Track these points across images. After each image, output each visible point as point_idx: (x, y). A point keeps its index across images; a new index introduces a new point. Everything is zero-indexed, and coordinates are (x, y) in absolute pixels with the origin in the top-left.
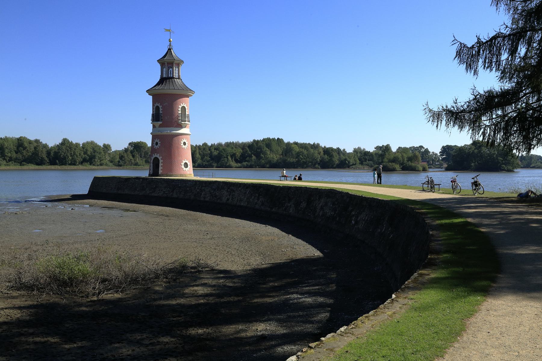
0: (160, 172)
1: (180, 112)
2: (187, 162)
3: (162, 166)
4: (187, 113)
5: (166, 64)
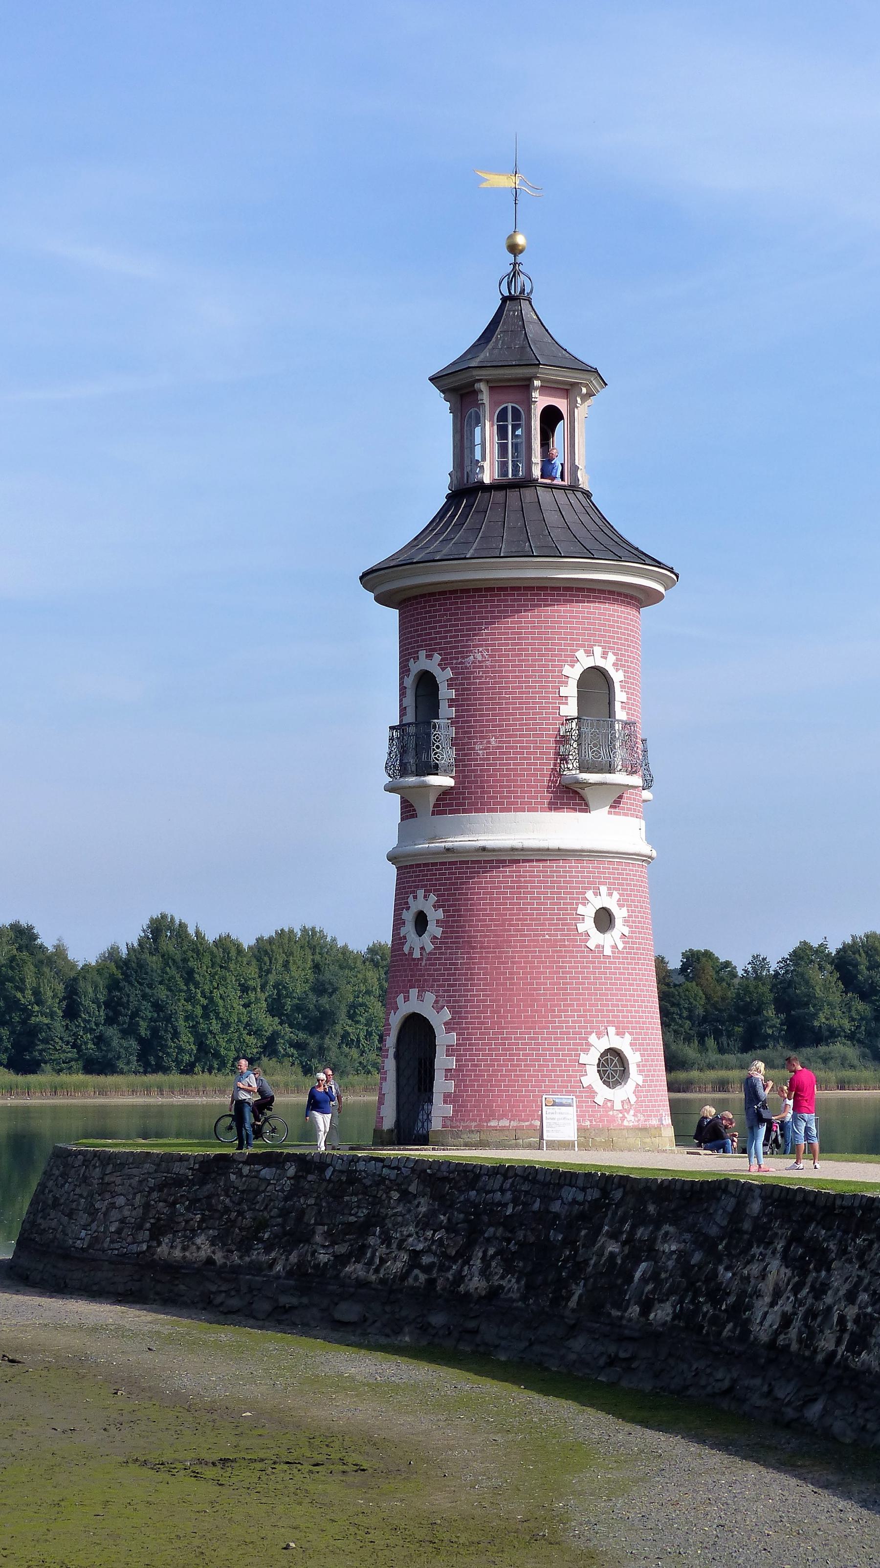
0: (440, 1110)
1: (571, 709)
2: (623, 1044)
4: (620, 714)
5: (485, 397)
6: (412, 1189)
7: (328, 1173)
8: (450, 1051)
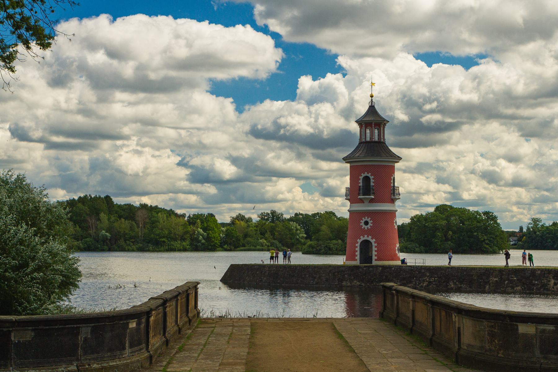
3: (376, 251)
7: (393, 269)
8: (376, 247)
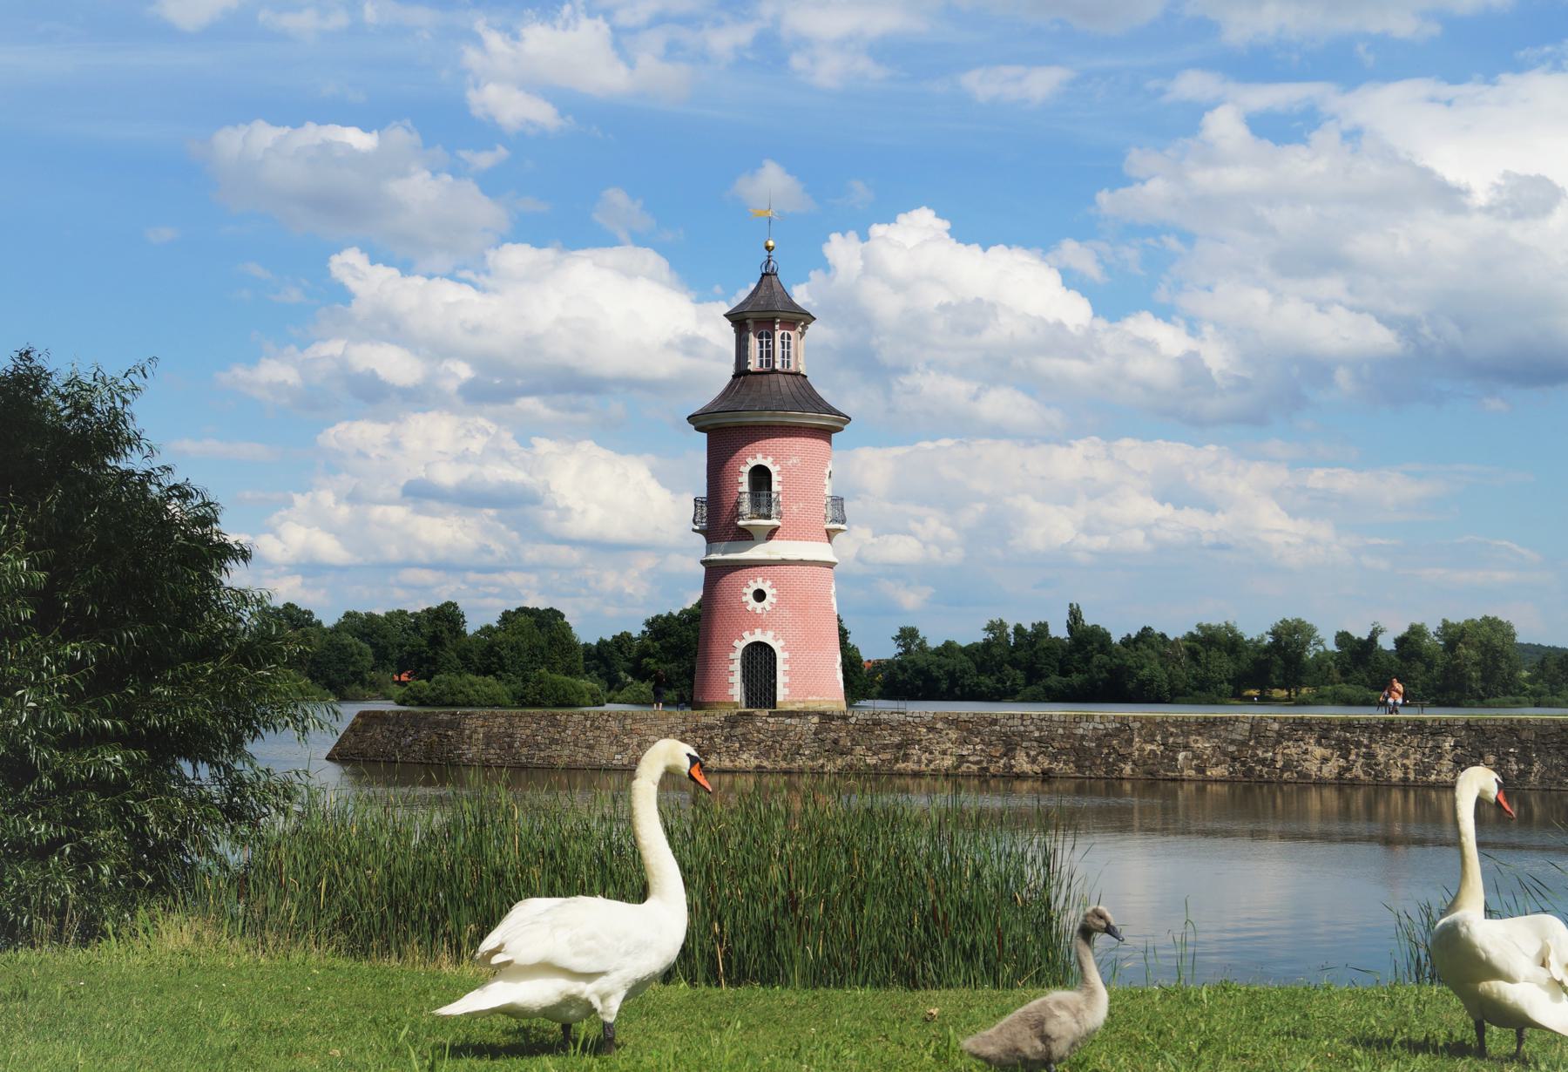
0: (782, 693)
6: (939, 725)
